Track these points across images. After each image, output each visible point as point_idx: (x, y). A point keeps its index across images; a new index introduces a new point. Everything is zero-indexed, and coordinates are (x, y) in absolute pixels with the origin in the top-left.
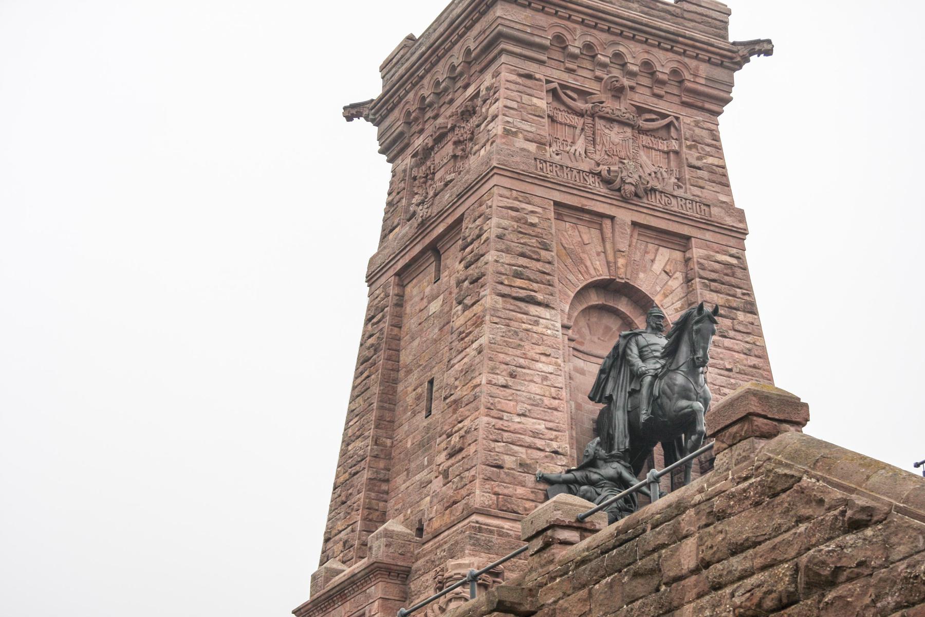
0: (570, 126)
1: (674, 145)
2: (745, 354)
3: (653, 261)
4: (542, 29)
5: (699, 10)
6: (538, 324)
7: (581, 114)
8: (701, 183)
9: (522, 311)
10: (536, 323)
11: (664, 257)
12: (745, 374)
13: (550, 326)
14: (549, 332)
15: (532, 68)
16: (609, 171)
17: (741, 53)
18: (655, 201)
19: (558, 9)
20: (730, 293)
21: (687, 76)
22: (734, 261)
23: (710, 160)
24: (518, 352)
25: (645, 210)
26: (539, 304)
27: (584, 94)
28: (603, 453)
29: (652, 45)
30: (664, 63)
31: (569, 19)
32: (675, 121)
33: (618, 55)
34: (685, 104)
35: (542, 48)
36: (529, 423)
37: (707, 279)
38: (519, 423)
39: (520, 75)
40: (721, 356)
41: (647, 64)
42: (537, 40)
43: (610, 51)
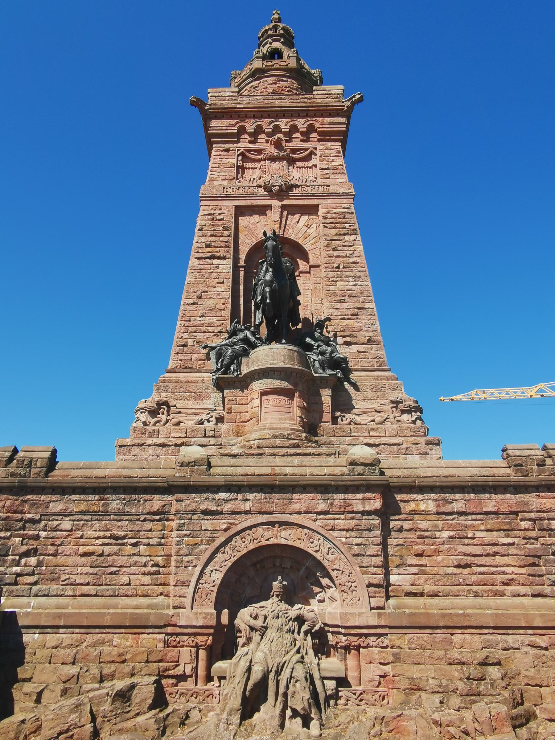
0: (254, 168)
2: (349, 257)
3: (298, 222)
5: (325, 92)
6: (218, 268)
7: (259, 161)
8: (327, 176)
9: (209, 263)
10: (217, 268)
11: (305, 218)
12: (349, 268)
13: (225, 268)
14: (224, 271)
15: (226, 146)
16: (265, 183)
17: (346, 105)
18: (296, 191)
19: (239, 114)
20: (341, 227)
21: (317, 125)
22: (345, 210)
23: (333, 163)
24: (203, 285)
26: (219, 258)
27: (259, 151)
30: (301, 123)
34: (319, 141)
37: (327, 223)
38: (200, 321)
39: (222, 151)
40: (333, 261)
42: (229, 131)
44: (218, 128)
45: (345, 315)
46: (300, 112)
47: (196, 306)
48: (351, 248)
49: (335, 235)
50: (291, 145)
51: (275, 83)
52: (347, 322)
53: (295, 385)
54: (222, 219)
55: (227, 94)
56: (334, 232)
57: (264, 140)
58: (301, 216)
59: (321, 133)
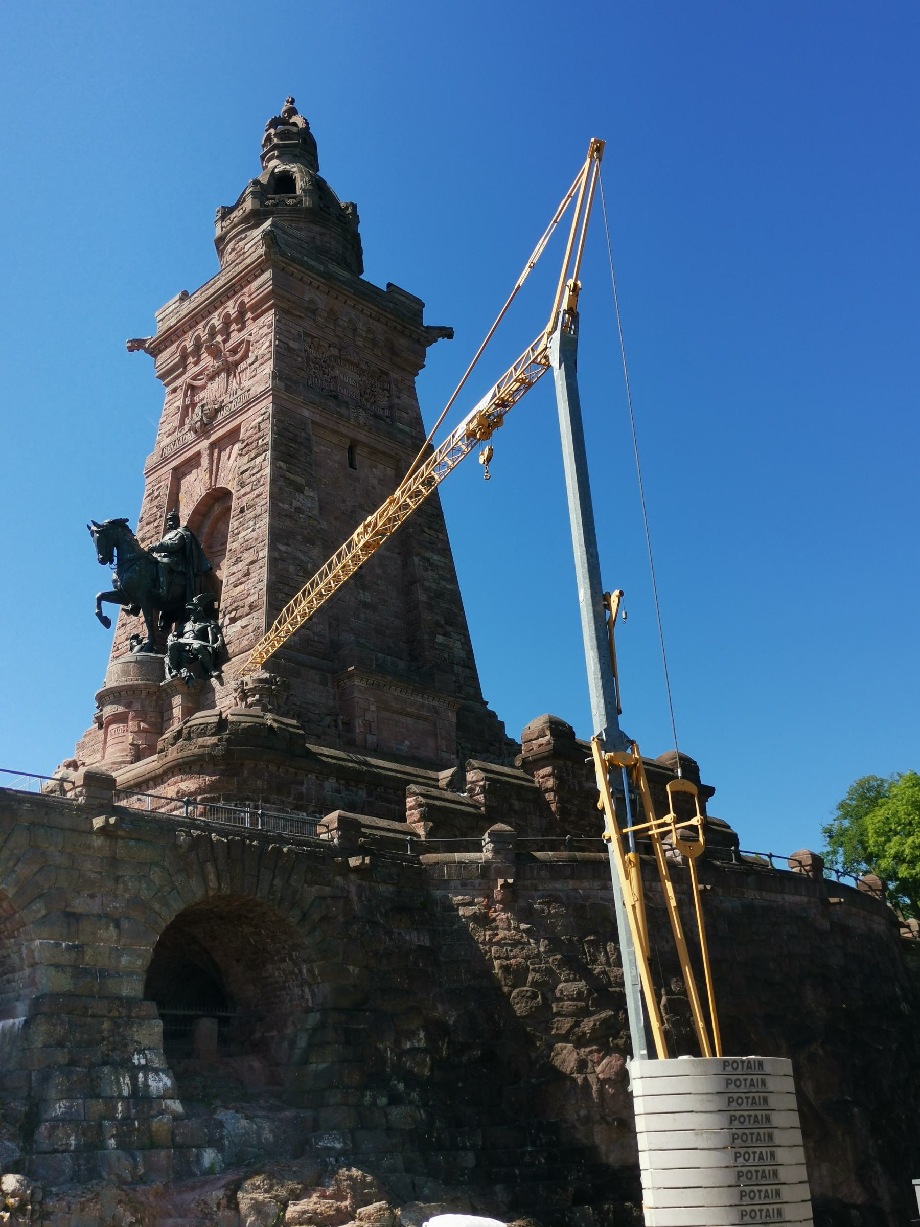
3: (229, 458)
8: (253, 374)
30: (231, 308)
44: (164, 365)
45: (239, 579)
46: (227, 293)
47: (124, 627)
48: (258, 475)
49: (248, 462)
50: (230, 345)
52: (240, 588)
53: (128, 705)
55: (171, 309)
56: (246, 458)
58: (232, 448)
59: (254, 308)
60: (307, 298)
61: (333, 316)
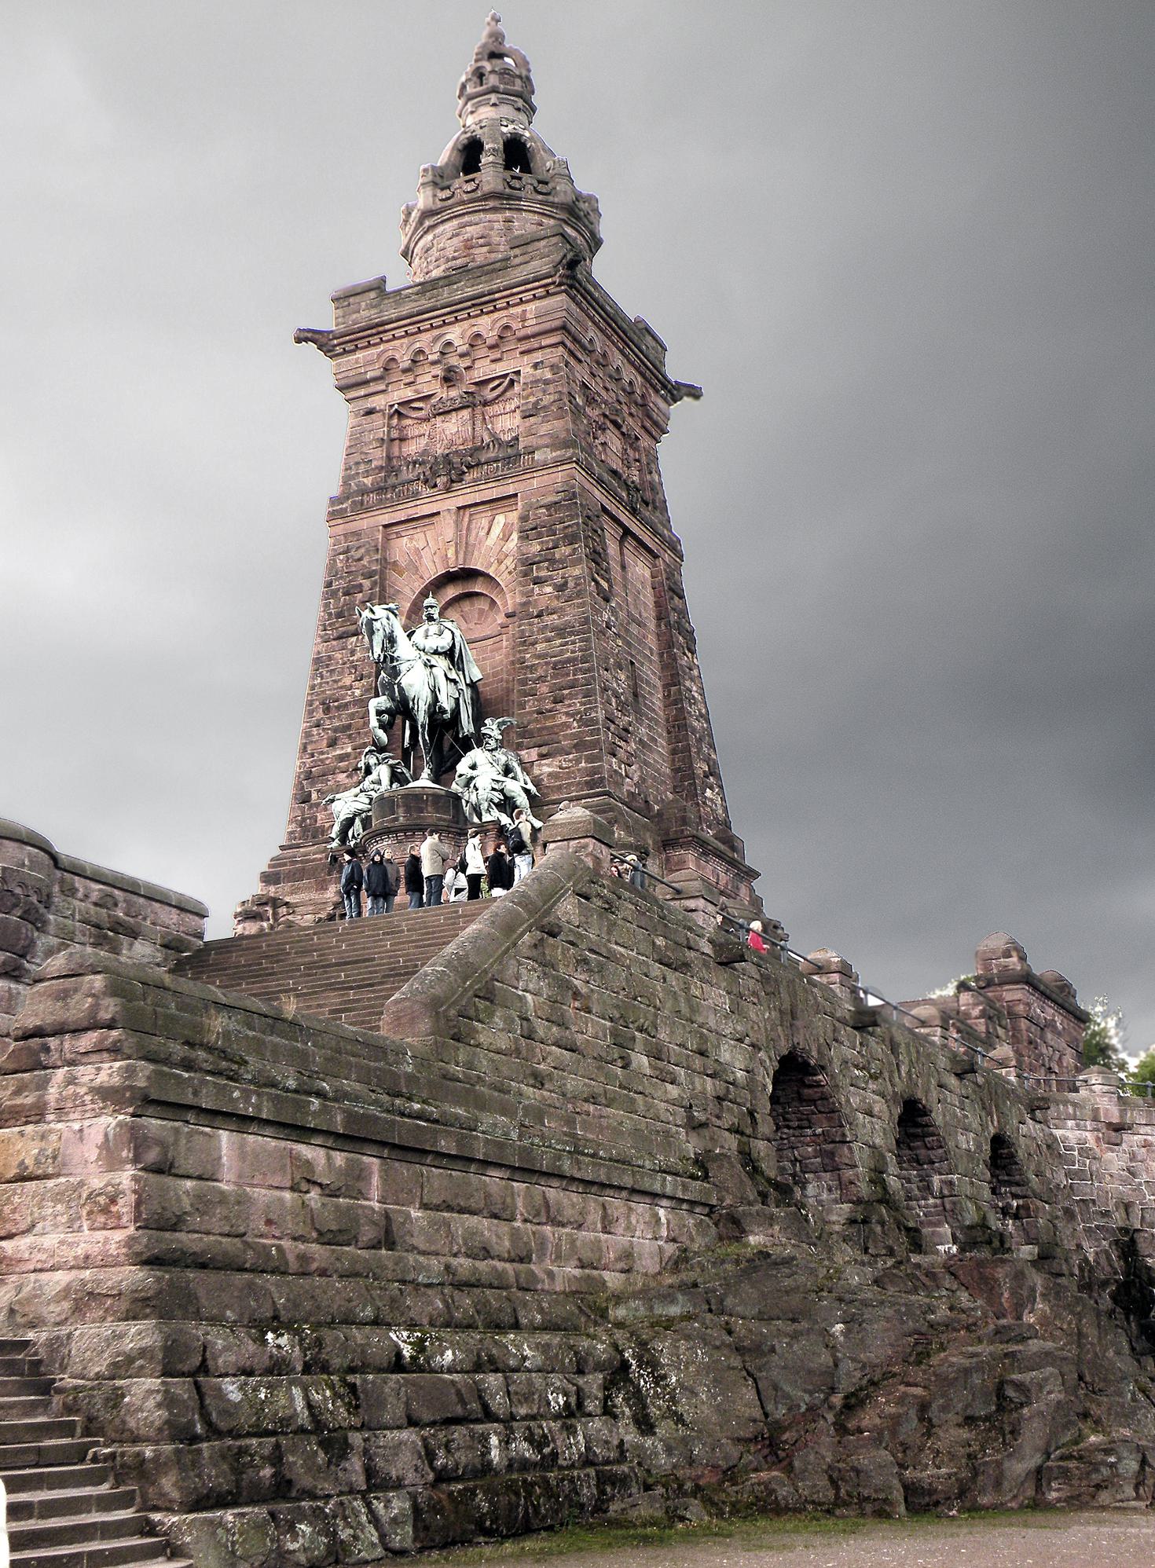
1: (516, 402)
3: (488, 533)
4: (371, 363)
10: (353, 653)
21: (515, 325)
25: (469, 490)
28: (372, 760)
29: (476, 316)
30: (487, 326)
31: (394, 338)
32: (515, 377)
33: (449, 344)
35: (375, 379)
36: (338, 752)
41: (478, 336)
43: (437, 347)
51: (457, 235)
54: (360, 559)
56: (535, 547)
57: (428, 377)
60: (591, 334)
61: (603, 362)
